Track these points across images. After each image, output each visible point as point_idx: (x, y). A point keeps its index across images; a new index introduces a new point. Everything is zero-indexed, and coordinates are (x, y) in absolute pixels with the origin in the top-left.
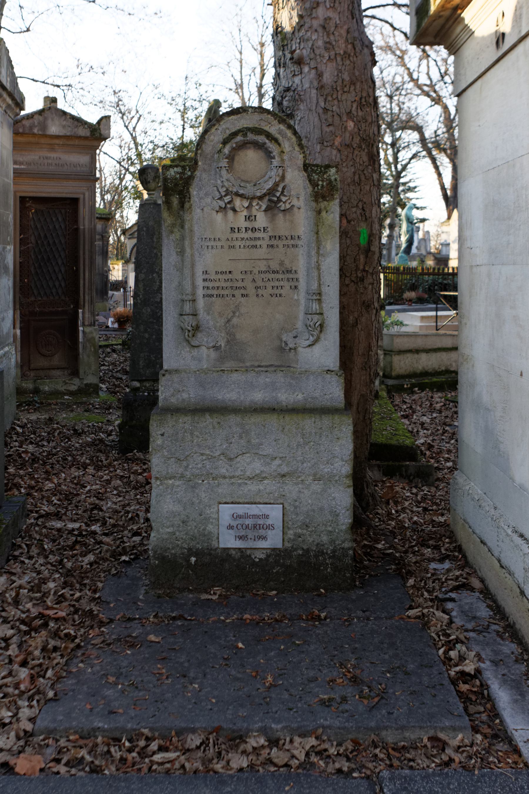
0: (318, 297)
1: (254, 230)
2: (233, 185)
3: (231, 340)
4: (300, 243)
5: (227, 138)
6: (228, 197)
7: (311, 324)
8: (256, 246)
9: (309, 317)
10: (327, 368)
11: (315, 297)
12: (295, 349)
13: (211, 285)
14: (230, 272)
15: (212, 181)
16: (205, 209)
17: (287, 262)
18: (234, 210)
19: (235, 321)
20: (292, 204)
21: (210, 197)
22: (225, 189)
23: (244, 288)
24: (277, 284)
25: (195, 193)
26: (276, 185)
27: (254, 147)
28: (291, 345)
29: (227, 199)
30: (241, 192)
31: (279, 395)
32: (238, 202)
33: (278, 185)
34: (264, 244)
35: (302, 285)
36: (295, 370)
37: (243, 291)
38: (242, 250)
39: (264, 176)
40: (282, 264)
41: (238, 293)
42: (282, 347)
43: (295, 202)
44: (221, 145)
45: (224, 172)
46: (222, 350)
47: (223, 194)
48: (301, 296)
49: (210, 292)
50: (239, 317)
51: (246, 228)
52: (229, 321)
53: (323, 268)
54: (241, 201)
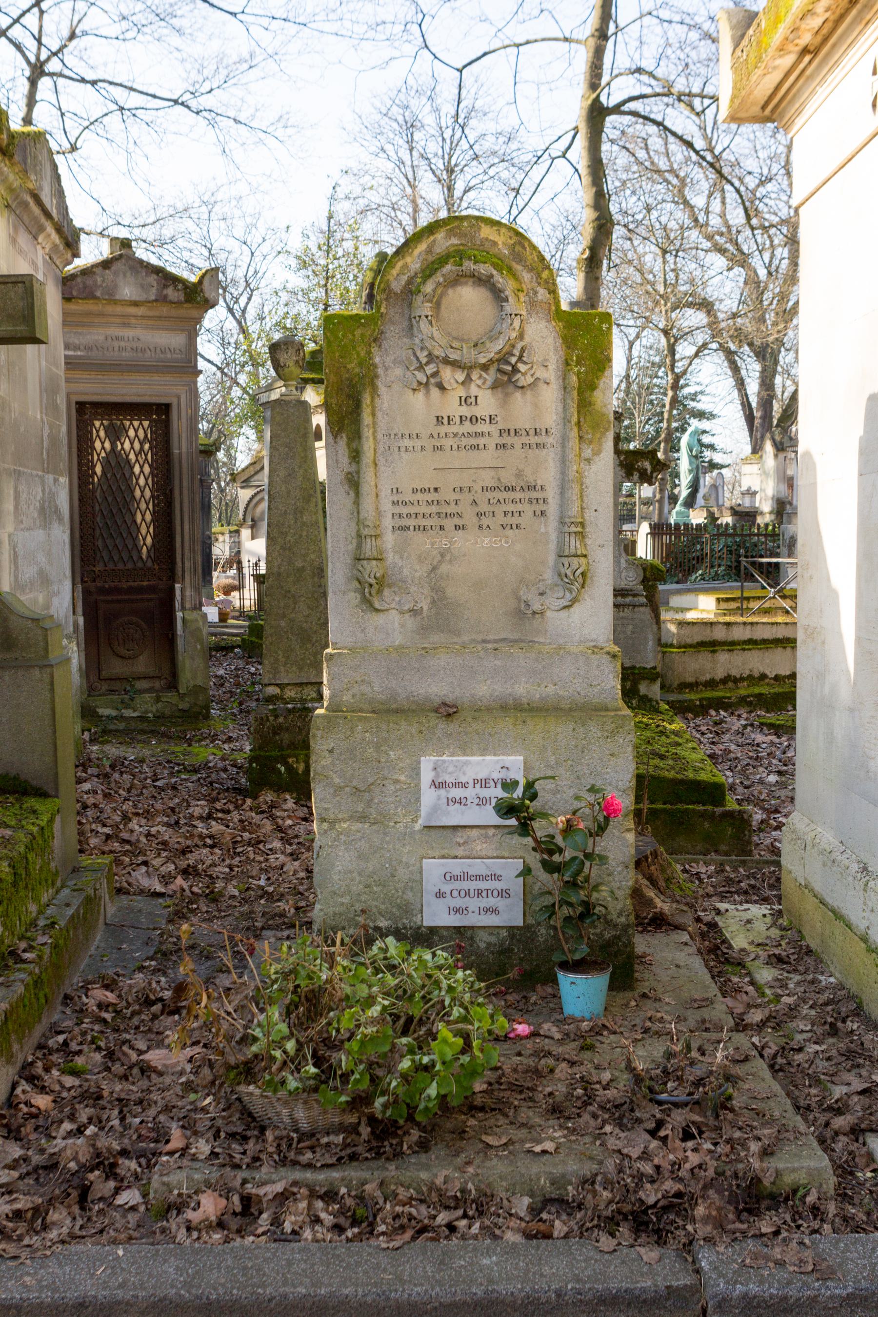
0: (579, 529)
1: (474, 420)
3: (439, 598)
4: (550, 440)
7: (569, 572)
8: (477, 447)
9: (566, 561)
12: (542, 613)
14: (436, 489)
18: (441, 387)
19: (444, 568)
23: (460, 516)
24: (511, 508)
28: (536, 607)
29: (430, 369)
30: (454, 356)
32: (447, 374)
33: (513, 346)
34: (491, 442)
35: (552, 509)
37: (457, 521)
38: (455, 453)
40: (519, 474)
41: (449, 523)
43: (540, 373)
47: (424, 360)
48: (551, 527)
50: (450, 561)
52: (434, 569)
53: (587, 481)
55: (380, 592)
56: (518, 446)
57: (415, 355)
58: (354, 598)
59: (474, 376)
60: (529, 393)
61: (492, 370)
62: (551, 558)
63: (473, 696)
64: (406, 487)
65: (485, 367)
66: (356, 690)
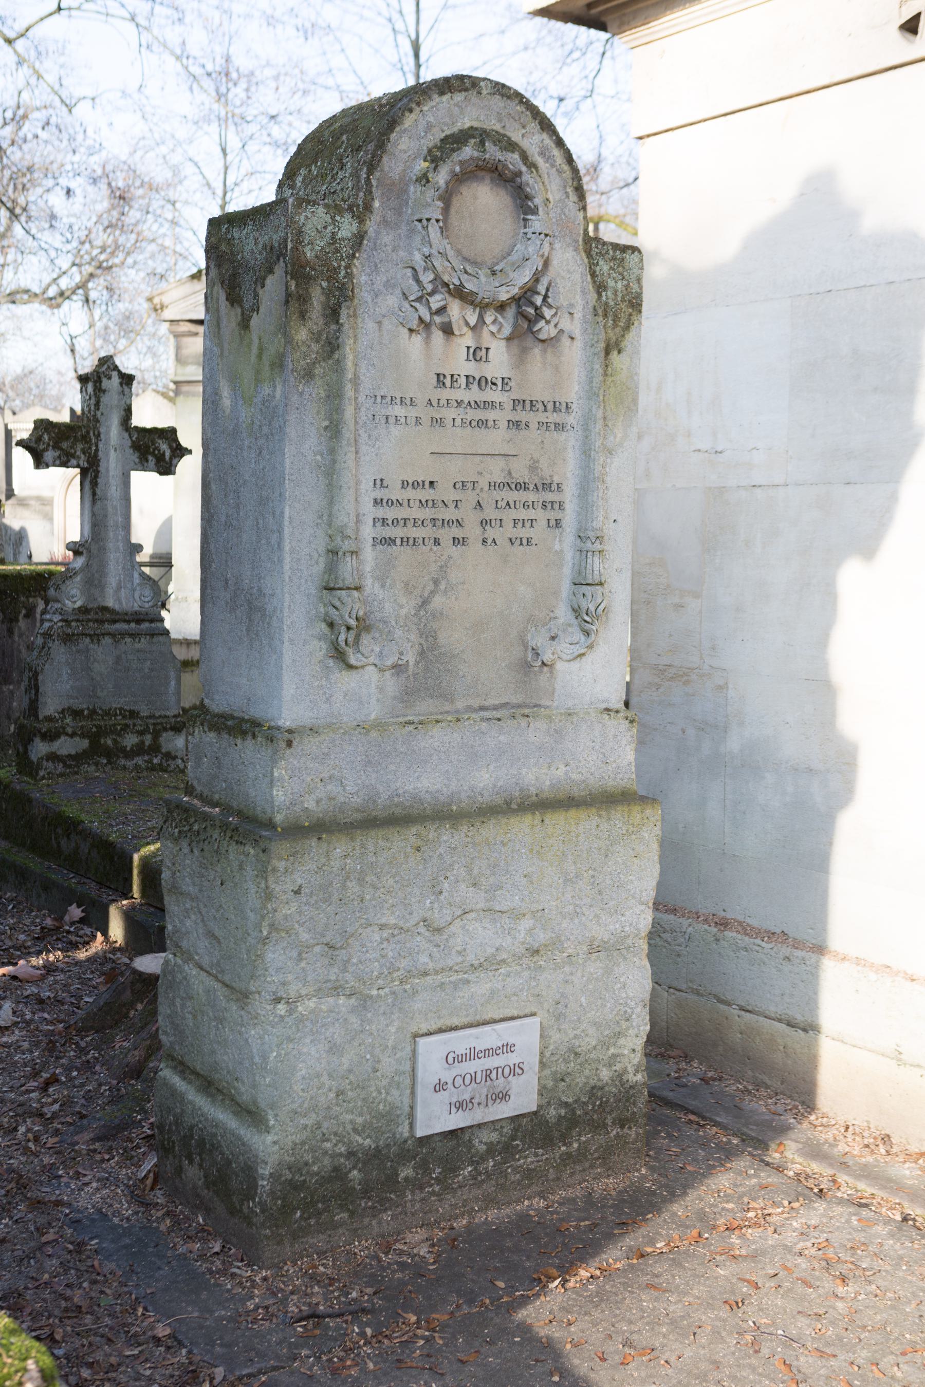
1: (483, 382)
2: (453, 268)
3: (430, 650)
4: (571, 420)
10: (604, 706)
12: (551, 666)
16: (386, 322)
17: (544, 464)
18: (448, 330)
19: (438, 602)
21: (398, 292)
22: (432, 277)
24: (523, 514)
27: (492, 180)
29: (436, 302)
32: (455, 310)
34: (501, 417)
36: (548, 712)
38: (458, 431)
40: (534, 467)
41: (445, 535)
42: (526, 662)
43: (565, 323)
45: (434, 231)
46: (410, 673)
47: (429, 287)
48: (566, 543)
49: (389, 532)
50: (446, 591)
52: (425, 602)
54: (462, 309)
56: (534, 425)
58: (320, 648)
59: (489, 319)
60: (550, 350)
61: (511, 312)
62: (566, 587)
63: (472, 789)
64: (394, 479)
65: (501, 307)
66: (320, 793)
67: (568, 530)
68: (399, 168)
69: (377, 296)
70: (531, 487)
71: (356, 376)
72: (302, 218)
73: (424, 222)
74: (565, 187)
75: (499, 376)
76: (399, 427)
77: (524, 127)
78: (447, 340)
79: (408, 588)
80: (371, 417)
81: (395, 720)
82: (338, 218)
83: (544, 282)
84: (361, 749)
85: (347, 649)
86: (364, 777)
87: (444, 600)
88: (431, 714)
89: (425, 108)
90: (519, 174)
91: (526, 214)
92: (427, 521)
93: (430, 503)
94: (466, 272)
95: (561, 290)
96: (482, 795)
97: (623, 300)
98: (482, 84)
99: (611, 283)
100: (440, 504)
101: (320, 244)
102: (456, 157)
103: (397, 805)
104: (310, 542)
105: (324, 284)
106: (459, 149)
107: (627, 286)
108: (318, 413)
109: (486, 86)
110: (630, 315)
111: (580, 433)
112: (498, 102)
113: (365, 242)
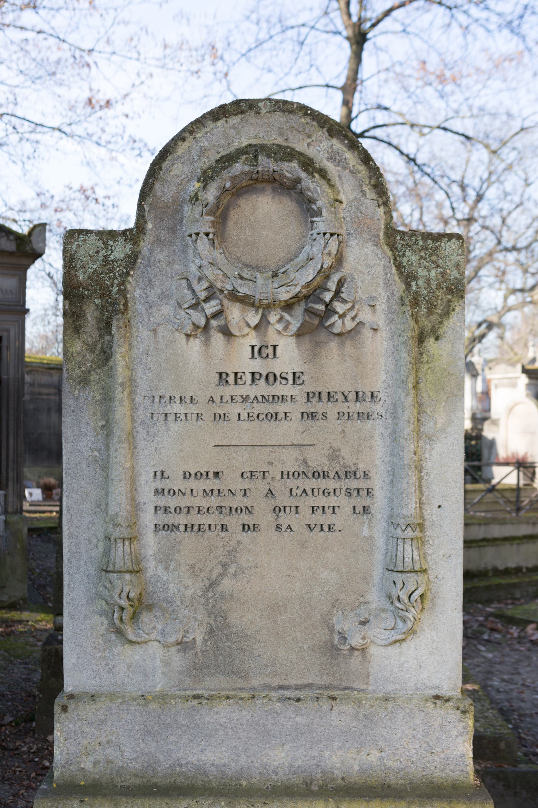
0: (418, 533)
1: (271, 378)
2: (225, 275)
4: (378, 408)
5: (211, 168)
6: (213, 303)
9: (399, 578)
10: (434, 692)
11: (409, 533)
12: (363, 650)
13: (172, 502)
14: (216, 474)
15: (176, 267)
18: (226, 332)
19: (227, 584)
20: (357, 320)
21: (173, 301)
22: (205, 285)
23: (249, 510)
24: (322, 501)
25: (138, 292)
26: (325, 274)
27: (274, 190)
29: (211, 307)
30: (244, 290)
31: (327, 753)
32: (235, 313)
33: (328, 278)
34: (295, 410)
35: (379, 503)
36: (361, 695)
37: (245, 518)
38: (244, 424)
39: (296, 256)
41: (234, 522)
42: (333, 645)
43: (365, 315)
44: (197, 185)
45: (203, 244)
46: (198, 649)
47: (203, 295)
48: (377, 529)
50: (235, 575)
51: (253, 374)
52: (213, 584)
53: (428, 466)
54: (243, 311)
55: (135, 617)
56: (332, 415)
57: (190, 287)
58: (101, 624)
59: (273, 318)
60: (348, 343)
61: (299, 310)
63: (265, 766)
64: (175, 472)
66: (99, 755)
67: (379, 516)
68: (173, 191)
69: (151, 307)
70: (332, 475)
71: (131, 380)
72: (74, 246)
73: (194, 236)
74: (361, 186)
75: (290, 370)
76: (178, 423)
77: (309, 136)
78: (228, 341)
79: (193, 571)
80: (149, 416)
81: (183, 693)
82: (110, 243)
83: (335, 278)
84: (138, 718)
85: (122, 626)
86: (143, 745)
87: (234, 582)
88: (223, 690)
89: (199, 135)
90: (299, 180)
91: (312, 217)
92: (212, 509)
93: (215, 493)
94: (241, 278)
95: (359, 284)
96: (277, 774)
97: (439, 287)
98: (260, 104)
99: (422, 272)
100: (226, 493)
101: (92, 267)
102: (225, 174)
103: (178, 775)
104: (89, 529)
105: (98, 301)
106: (230, 166)
107: (443, 274)
108: (94, 414)
109: (265, 105)
110: (450, 301)
111: (390, 420)
112: (279, 118)
113: (139, 260)
